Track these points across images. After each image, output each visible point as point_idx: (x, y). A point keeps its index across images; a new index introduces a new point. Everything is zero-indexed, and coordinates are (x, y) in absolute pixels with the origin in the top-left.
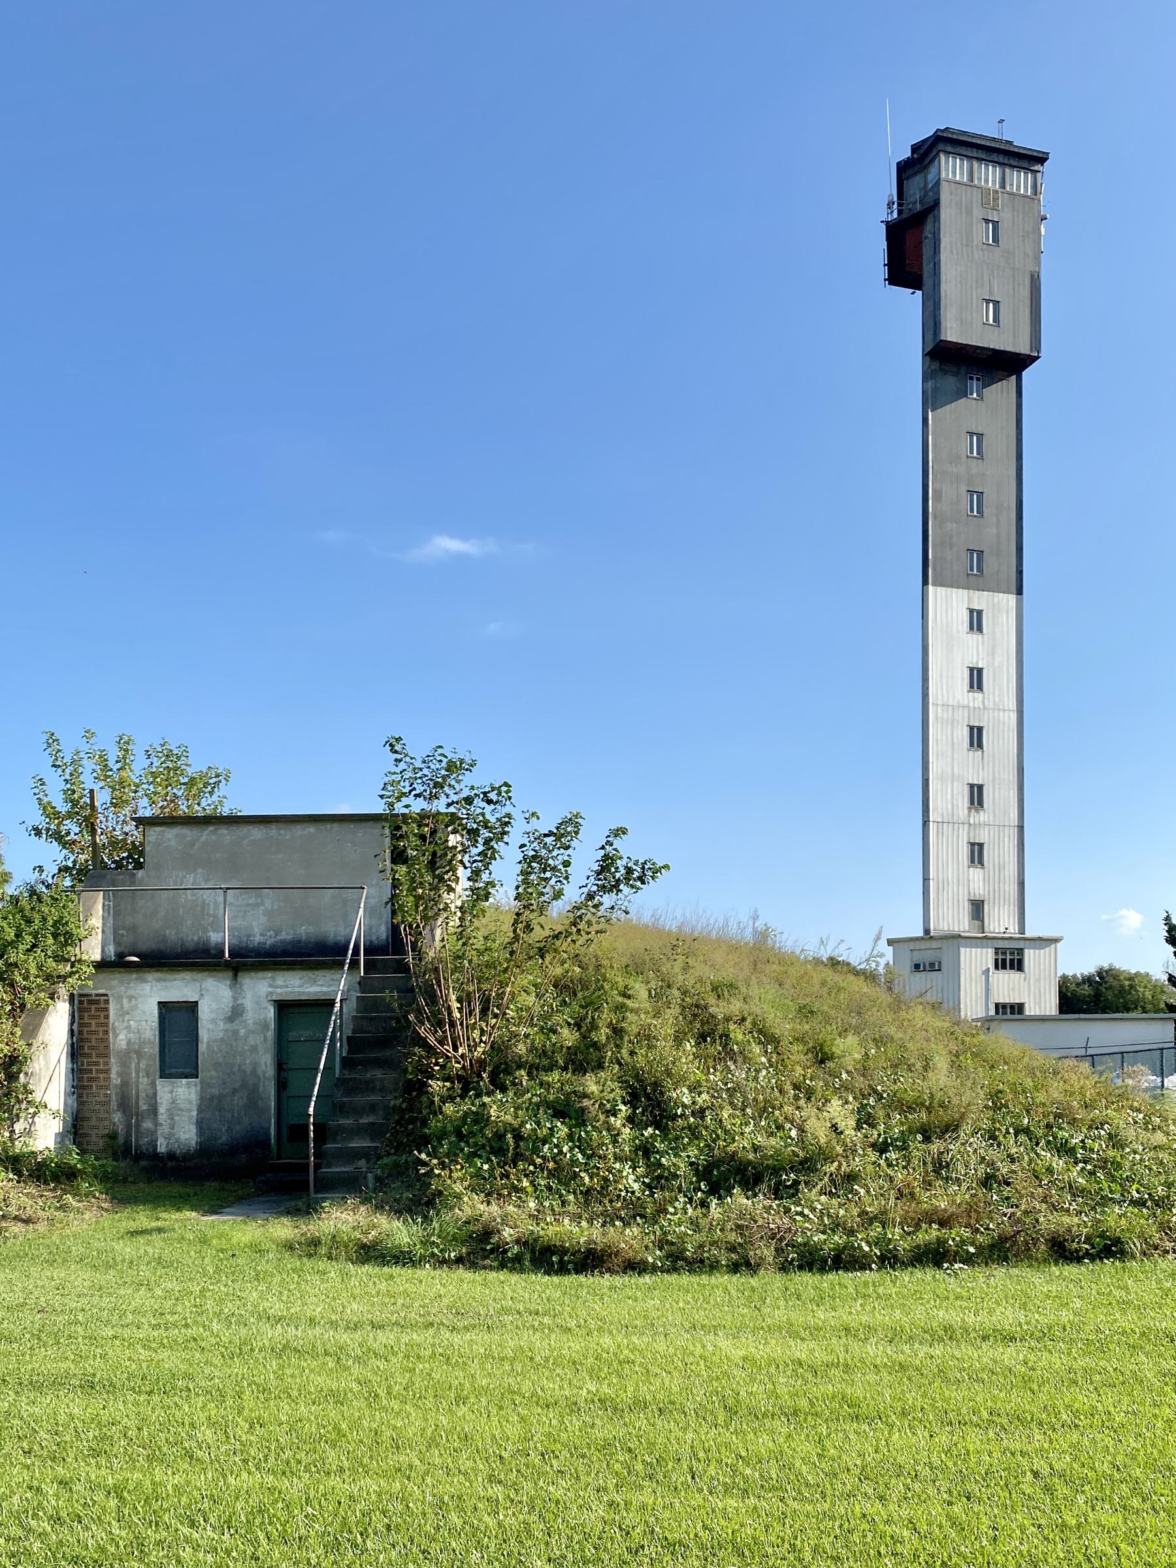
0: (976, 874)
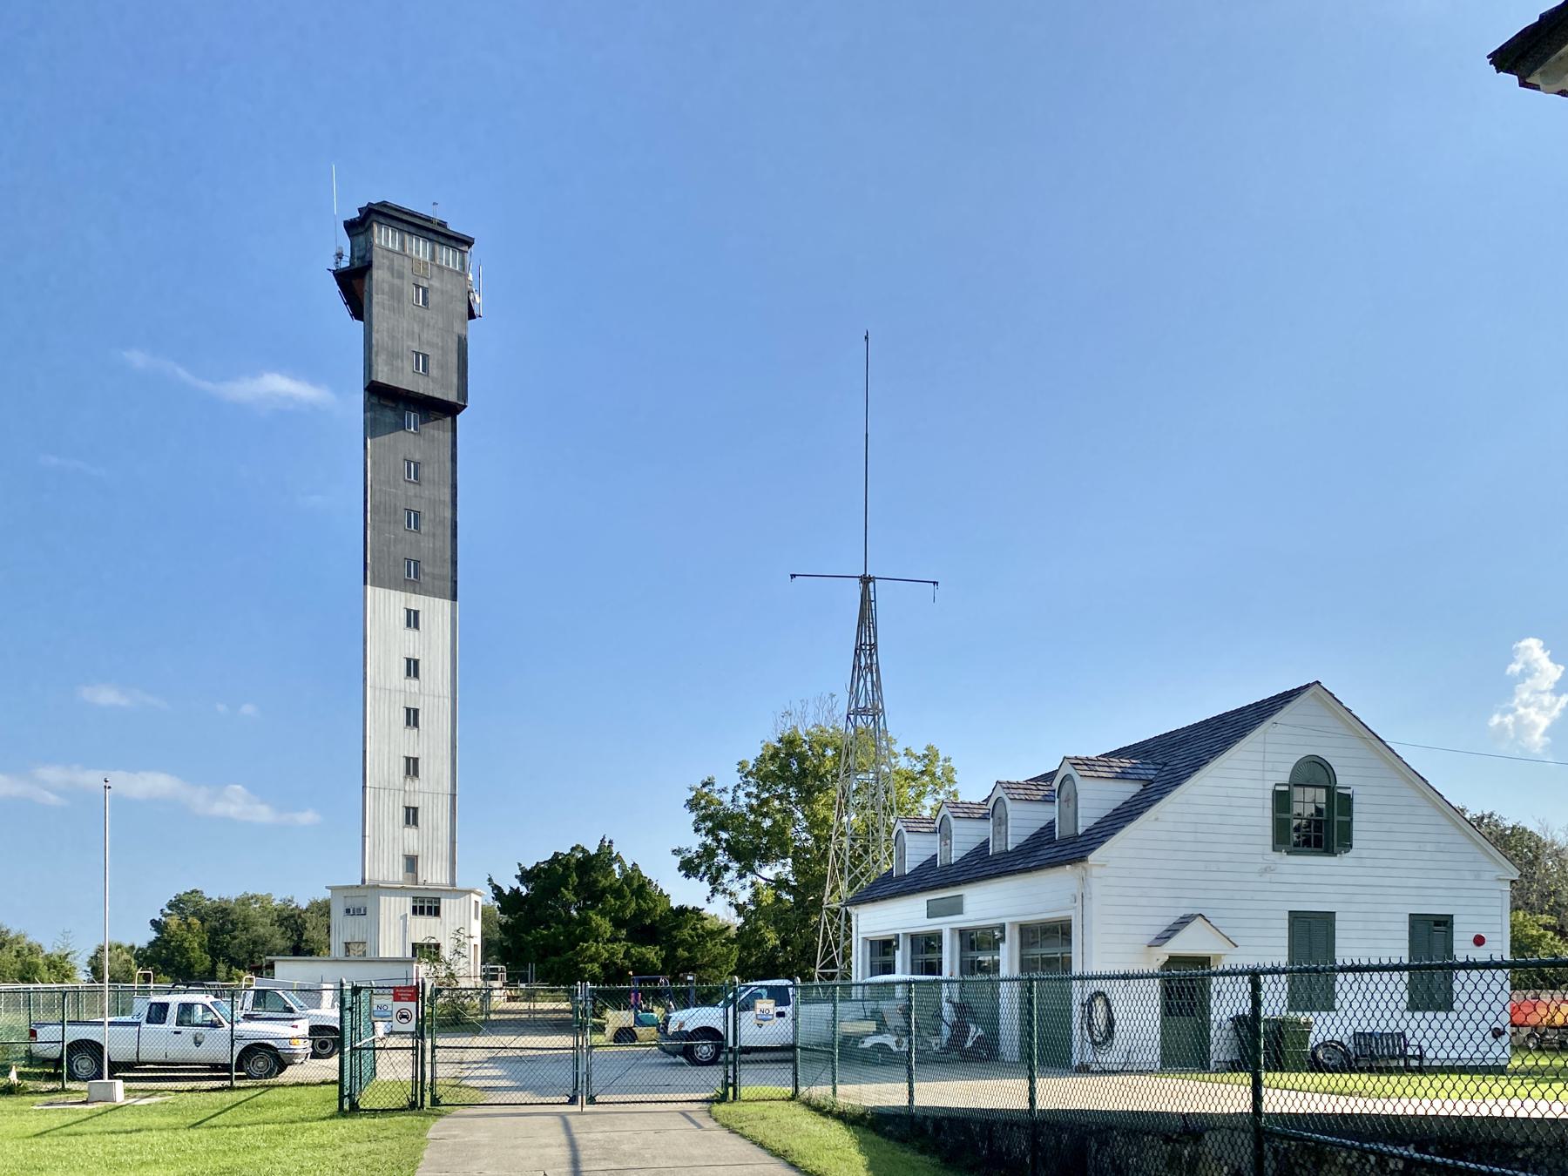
0: (411, 832)
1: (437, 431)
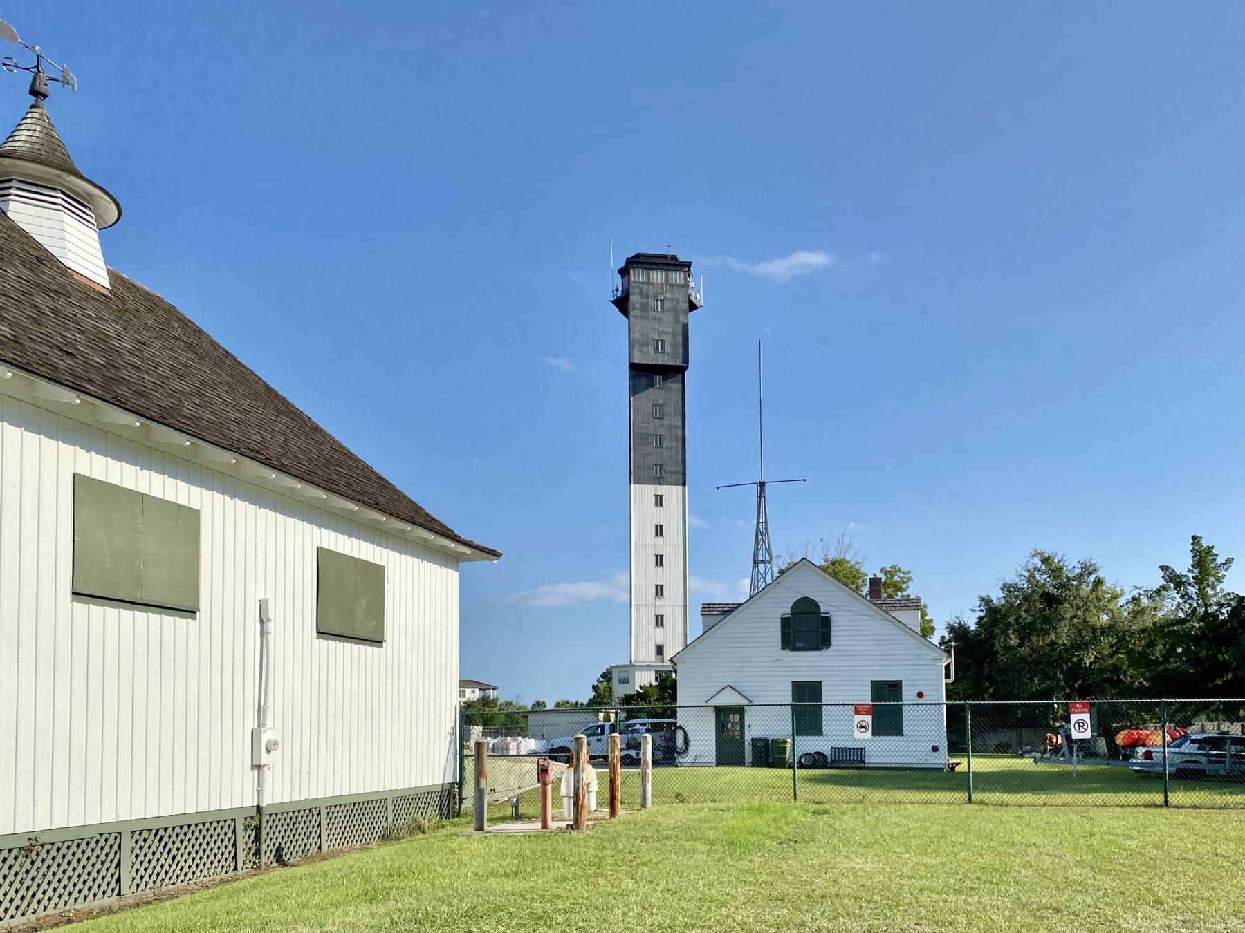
0: (659, 630)
1: (674, 386)
